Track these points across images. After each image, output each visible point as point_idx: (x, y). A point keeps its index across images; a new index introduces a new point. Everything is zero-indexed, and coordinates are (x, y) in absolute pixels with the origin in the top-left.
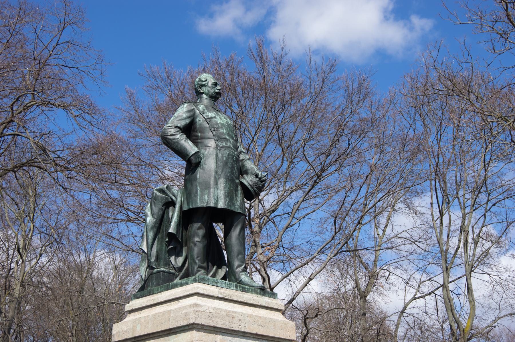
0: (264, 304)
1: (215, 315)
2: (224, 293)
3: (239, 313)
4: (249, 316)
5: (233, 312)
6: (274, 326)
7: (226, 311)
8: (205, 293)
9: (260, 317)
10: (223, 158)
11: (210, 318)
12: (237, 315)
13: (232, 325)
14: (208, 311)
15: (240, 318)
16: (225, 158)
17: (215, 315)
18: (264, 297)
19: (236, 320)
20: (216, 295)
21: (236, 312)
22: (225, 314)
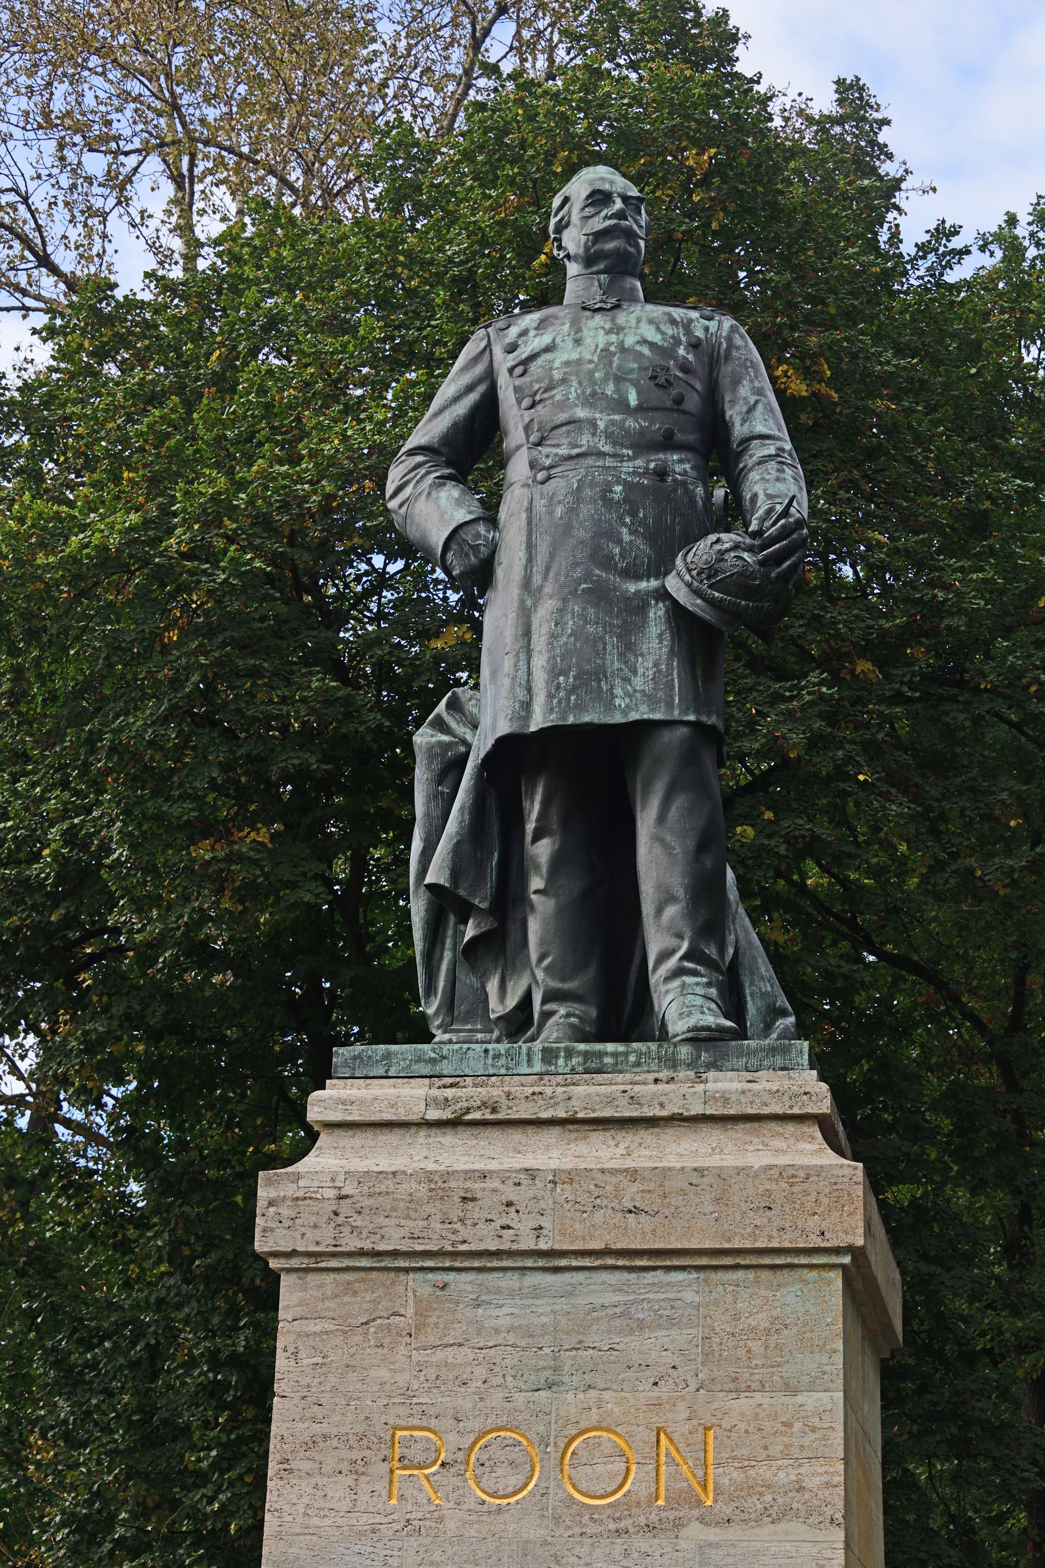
0: (697, 1109)
1: (368, 1202)
2: (457, 1099)
3: (504, 1177)
4: (571, 1177)
5: (468, 1174)
6: (717, 1201)
7: (429, 1176)
8: (355, 1117)
9: (633, 1174)
10: (551, 513)
11: (340, 1220)
12: (496, 1184)
13: (464, 1232)
14: (331, 1193)
15: (510, 1193)
16: (559, 511)
17: (368, 1202)
18: (711, 1074)
19: (488, 1205)
20: (414, 1117)
21: (484, 1176)
22: (424, 1188)
